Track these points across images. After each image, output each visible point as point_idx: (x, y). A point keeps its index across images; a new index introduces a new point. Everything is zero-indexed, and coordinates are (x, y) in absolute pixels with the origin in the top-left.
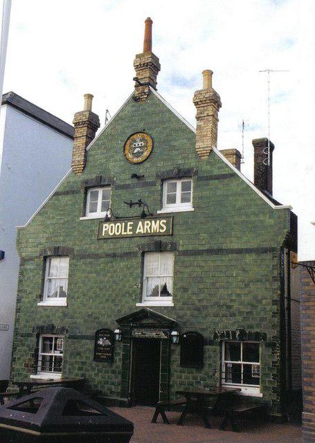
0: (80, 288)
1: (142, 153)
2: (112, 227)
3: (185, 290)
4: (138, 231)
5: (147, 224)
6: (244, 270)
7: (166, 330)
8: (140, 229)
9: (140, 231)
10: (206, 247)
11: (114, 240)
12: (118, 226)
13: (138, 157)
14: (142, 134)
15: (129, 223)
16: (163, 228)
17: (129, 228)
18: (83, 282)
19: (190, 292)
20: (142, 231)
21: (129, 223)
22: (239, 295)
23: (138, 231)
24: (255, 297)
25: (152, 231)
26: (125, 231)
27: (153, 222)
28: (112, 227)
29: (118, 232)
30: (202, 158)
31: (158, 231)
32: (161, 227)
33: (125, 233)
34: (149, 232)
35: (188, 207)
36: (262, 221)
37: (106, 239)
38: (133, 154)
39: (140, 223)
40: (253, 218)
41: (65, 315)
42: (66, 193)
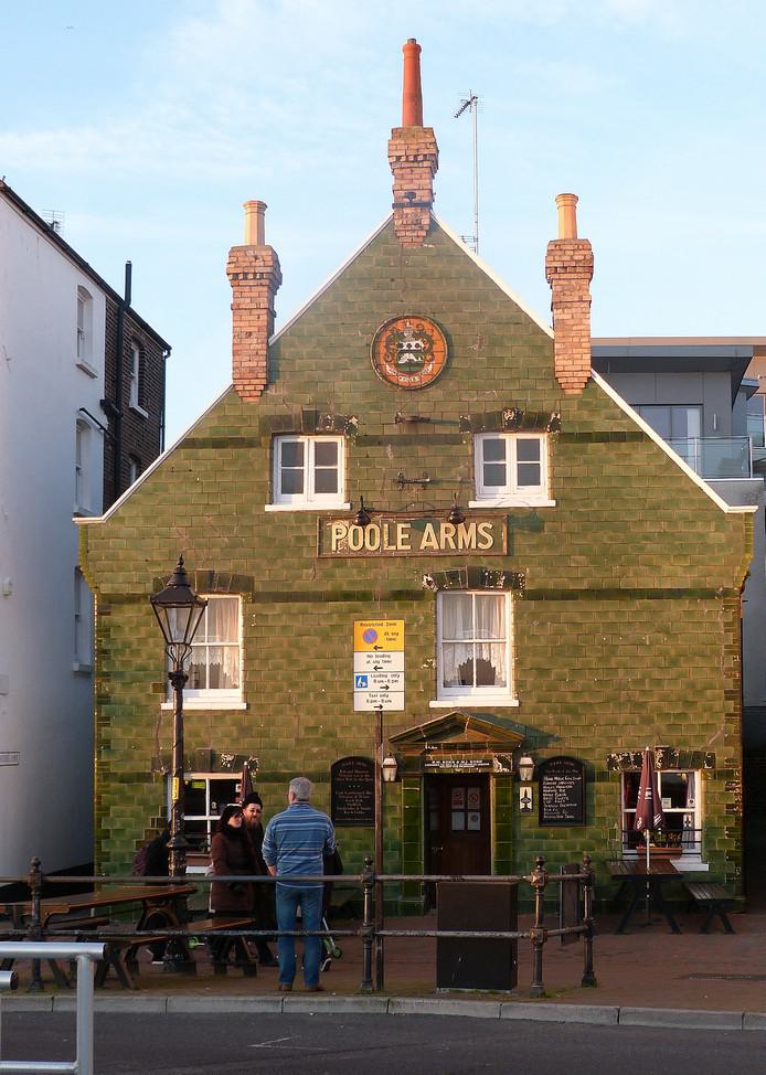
0: (277, 668)
1: (420, 365)
6: (667, 633)
7: (503, 755)
10: (584, 586)
11: (364, 563)
12: (372, 531)
14: (417, 322)
18: (287, 656)
22: (658, 682)
24: (692, 685)
25: (461, 547)
33: (393, 548)
36: (701, 536)
40: (682, 528)
42: (218, 444)
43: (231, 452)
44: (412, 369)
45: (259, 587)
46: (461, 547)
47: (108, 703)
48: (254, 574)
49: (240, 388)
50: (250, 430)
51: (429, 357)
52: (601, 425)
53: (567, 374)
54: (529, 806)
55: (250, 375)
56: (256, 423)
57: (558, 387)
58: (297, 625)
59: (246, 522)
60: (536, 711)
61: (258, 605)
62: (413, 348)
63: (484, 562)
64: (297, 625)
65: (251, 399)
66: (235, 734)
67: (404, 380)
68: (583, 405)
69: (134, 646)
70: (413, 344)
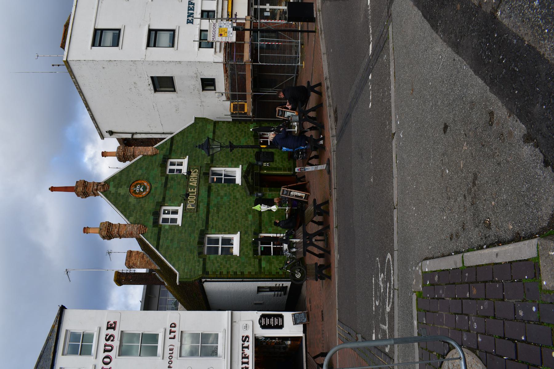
1: (144, 186)
2: (189, 202)
3: (232, 160)
4: (195, 185)
5: (192, 179)
8: (194, 184)
9: (195, 184)
13: (146, 188)
15: (190, 191)
16: (196, 171)
17: (192, 191)
19: (234, 158)
20: (195, 183)
21: (190, 191)
22: (236, 137)
23: (195, 185)
25: (197, 176)
26: (194, 193)
27: (191, 176)
28: (189, 202)
29: (194, 198)
30: (158, 153)
31: (197, 174)
32: (195, 172)
33: (195, 192)
34: (197, 178)
35: (185, 161)
37: (198, 206)
38: (143, 191)
39: (191, 184)
41: (246, 233)
42: (159, 239)
43: (162, 236)
44: (145, 188)
45: (203, 228)
46: (197, 176)
47: (237, 272)
48: (200, 229)
49: (143, 232)
50: (156, 230)
51: (142, 184)
52: (168, 146)
53: (153, 151)
54: (268, 164)
55: (139, 229)
56: (154, 228)
57: (156, 154)
58: (216, 218)
59: (183, 231)
60: (243, 161)
61: (209, 228)
62: (139, 188)
63: (202, 172)
64: (216, 218)
65: (147, 230)
66: (247, 235)
67: (148, 190)
68: (162, 150)
69: (219, 264)
70: (138, 188)
